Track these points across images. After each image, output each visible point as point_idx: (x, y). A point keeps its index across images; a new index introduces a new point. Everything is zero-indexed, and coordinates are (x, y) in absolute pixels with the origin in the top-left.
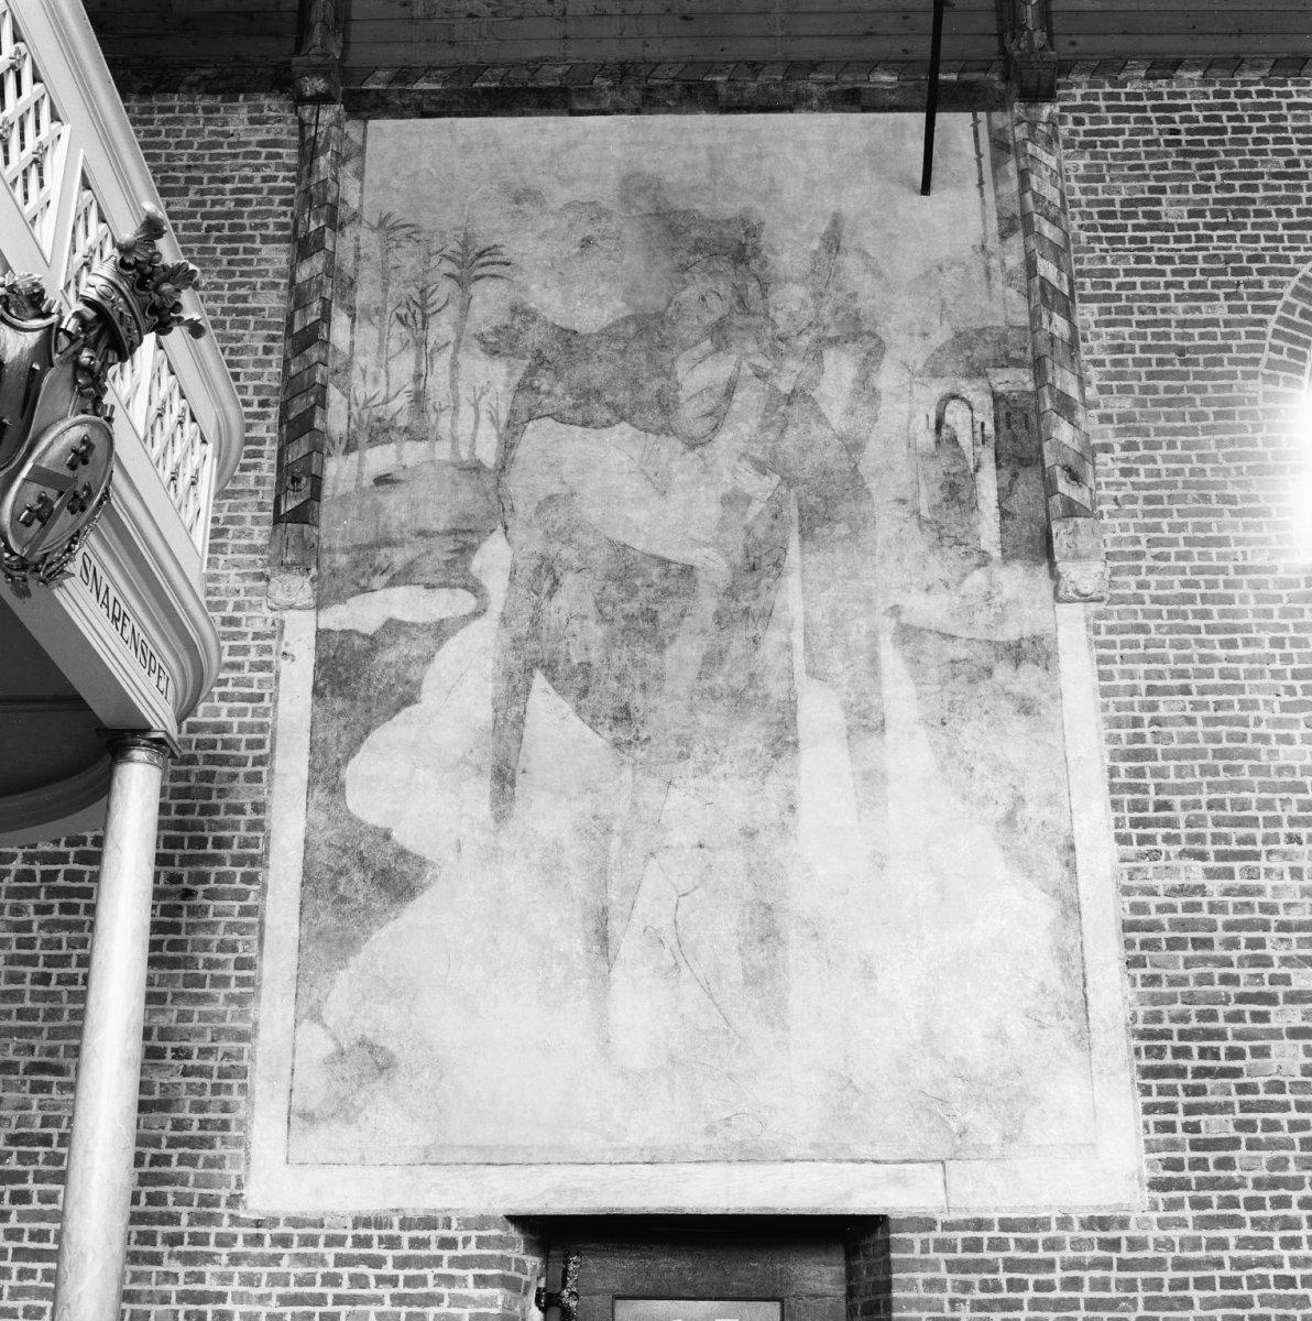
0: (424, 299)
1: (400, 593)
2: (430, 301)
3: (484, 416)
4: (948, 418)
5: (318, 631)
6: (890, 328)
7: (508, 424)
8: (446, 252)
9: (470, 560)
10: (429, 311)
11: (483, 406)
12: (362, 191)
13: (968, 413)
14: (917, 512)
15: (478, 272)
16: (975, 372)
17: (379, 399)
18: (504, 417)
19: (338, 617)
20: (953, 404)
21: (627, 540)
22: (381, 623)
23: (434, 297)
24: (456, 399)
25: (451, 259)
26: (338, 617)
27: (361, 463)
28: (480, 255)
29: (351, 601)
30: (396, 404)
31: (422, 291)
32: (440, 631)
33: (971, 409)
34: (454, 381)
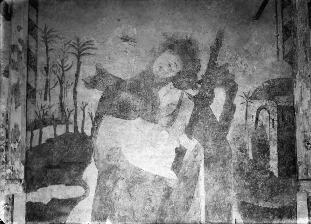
0: (63, 64)
1: (55, 188)
2: (65, 65)
3: (87, 115)
4: (260, 117)
5: (26, 203)
6: (239, 79)
7: (97, 118)
8: (71, 43)
9: (82, 174)
10: (65, 69)
11: (86, 110)
12: (37, 16)
13: (268, 115)
14: (246, 156)
15: (84, 52)
16: (271, 98)
17: (47, 107)
18: (94, 115)
19: (34, 197)
20: (262, 111)
21: (140, 167)
22: (50, 200)
23: (67, 63)
24: (76, 107)
25: (73, 46)
26: (34, 197)
27: (41, 133)
28: (84, 45)
29: (39, 190)
30: (53, 109)
31: (62, 61)
32: (72, 202)
33: (269, 113)
34: (75, 98)
